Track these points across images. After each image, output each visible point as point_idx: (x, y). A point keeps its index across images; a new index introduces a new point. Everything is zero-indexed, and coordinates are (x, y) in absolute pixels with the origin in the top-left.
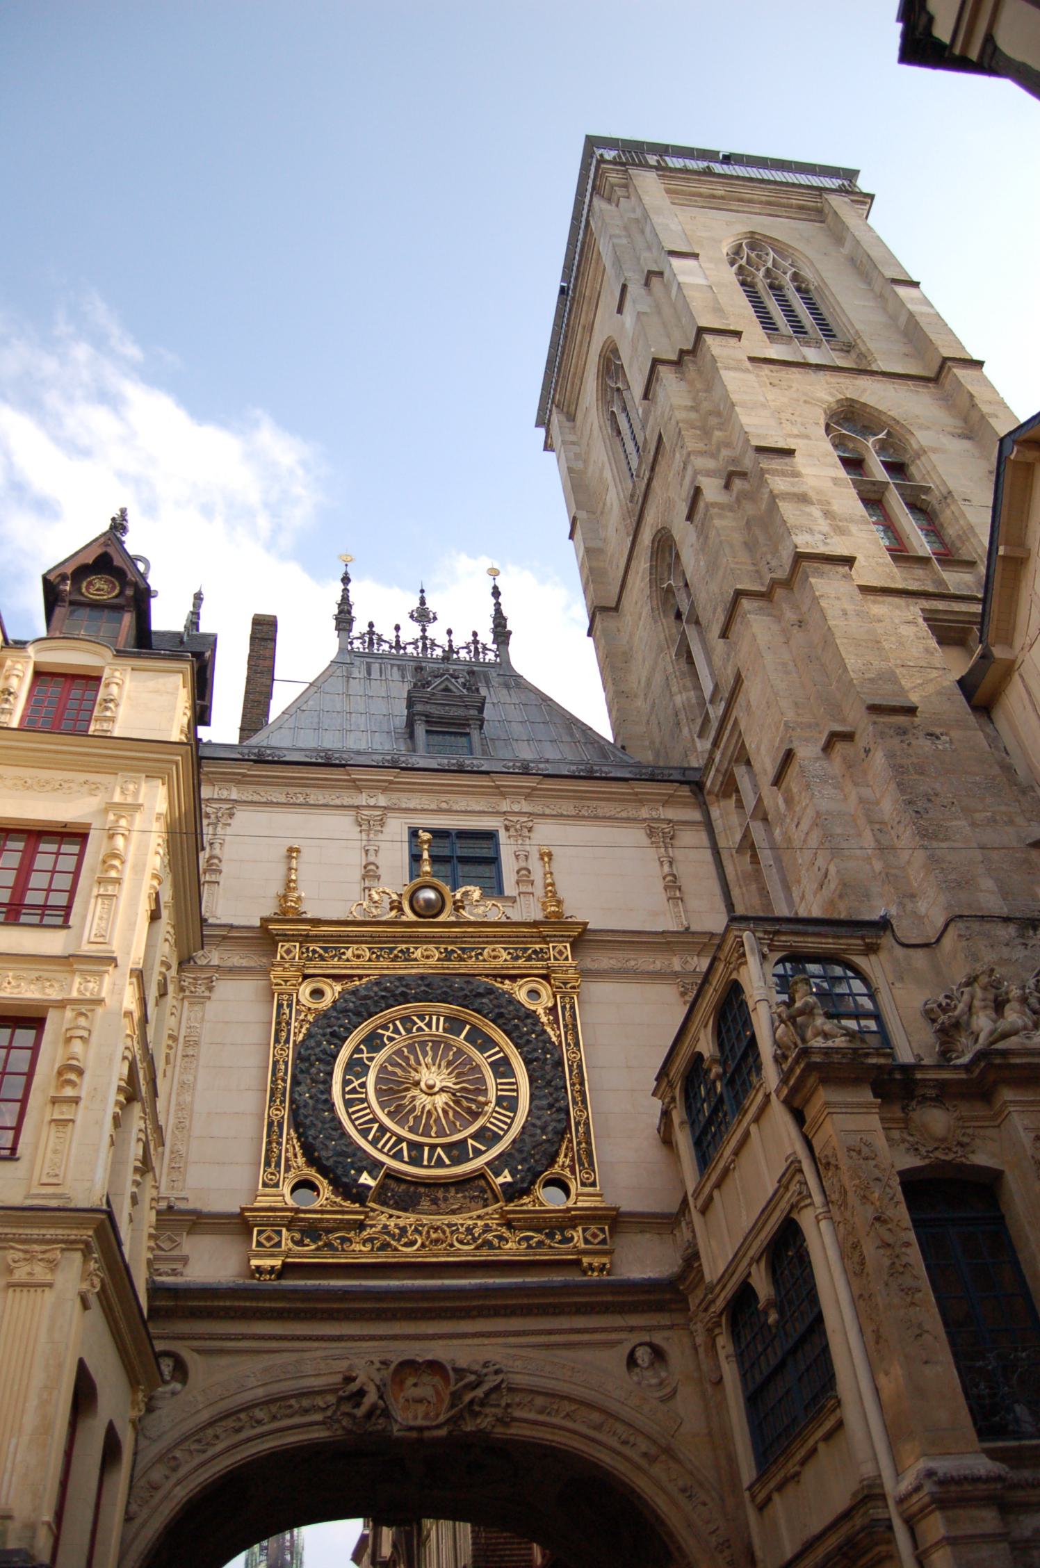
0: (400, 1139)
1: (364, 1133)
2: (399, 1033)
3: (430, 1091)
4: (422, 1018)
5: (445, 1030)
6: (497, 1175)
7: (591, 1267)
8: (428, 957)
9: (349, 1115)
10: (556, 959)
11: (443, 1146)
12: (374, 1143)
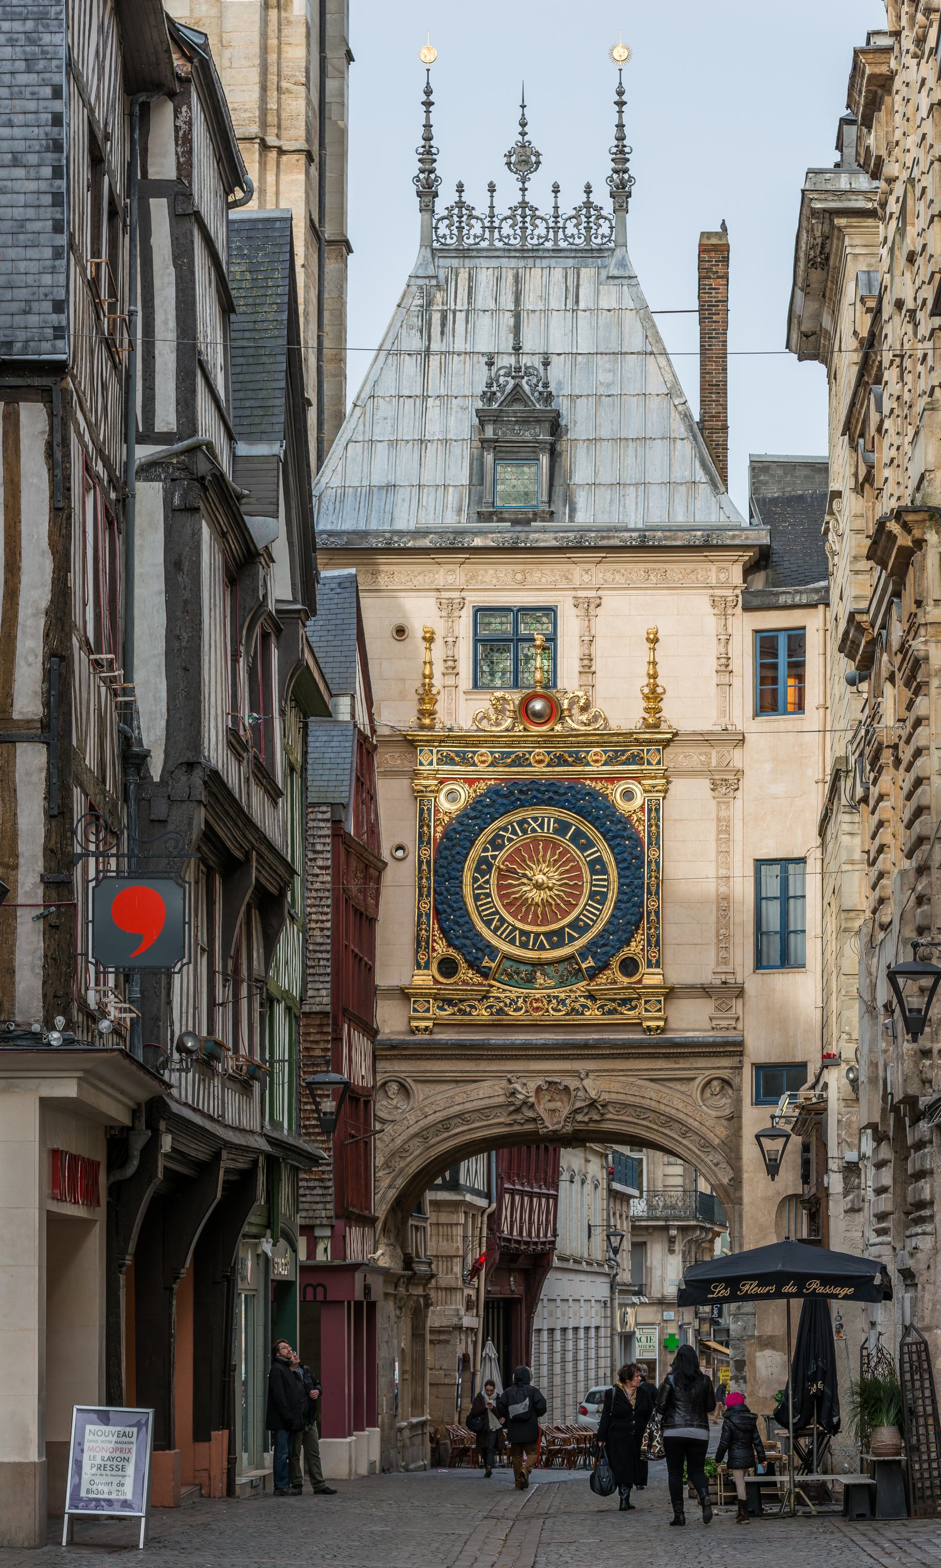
0: (515, 928)
1: (488, 923)
2: (516, 834)
3: (539, 886)
4: (535, 819)
6: (584, 959)
7: (649, 1029)
8: (540, 762)
9: (477, 907)
10: (649, 763)
11: (545, 934)
12: (494, 931)
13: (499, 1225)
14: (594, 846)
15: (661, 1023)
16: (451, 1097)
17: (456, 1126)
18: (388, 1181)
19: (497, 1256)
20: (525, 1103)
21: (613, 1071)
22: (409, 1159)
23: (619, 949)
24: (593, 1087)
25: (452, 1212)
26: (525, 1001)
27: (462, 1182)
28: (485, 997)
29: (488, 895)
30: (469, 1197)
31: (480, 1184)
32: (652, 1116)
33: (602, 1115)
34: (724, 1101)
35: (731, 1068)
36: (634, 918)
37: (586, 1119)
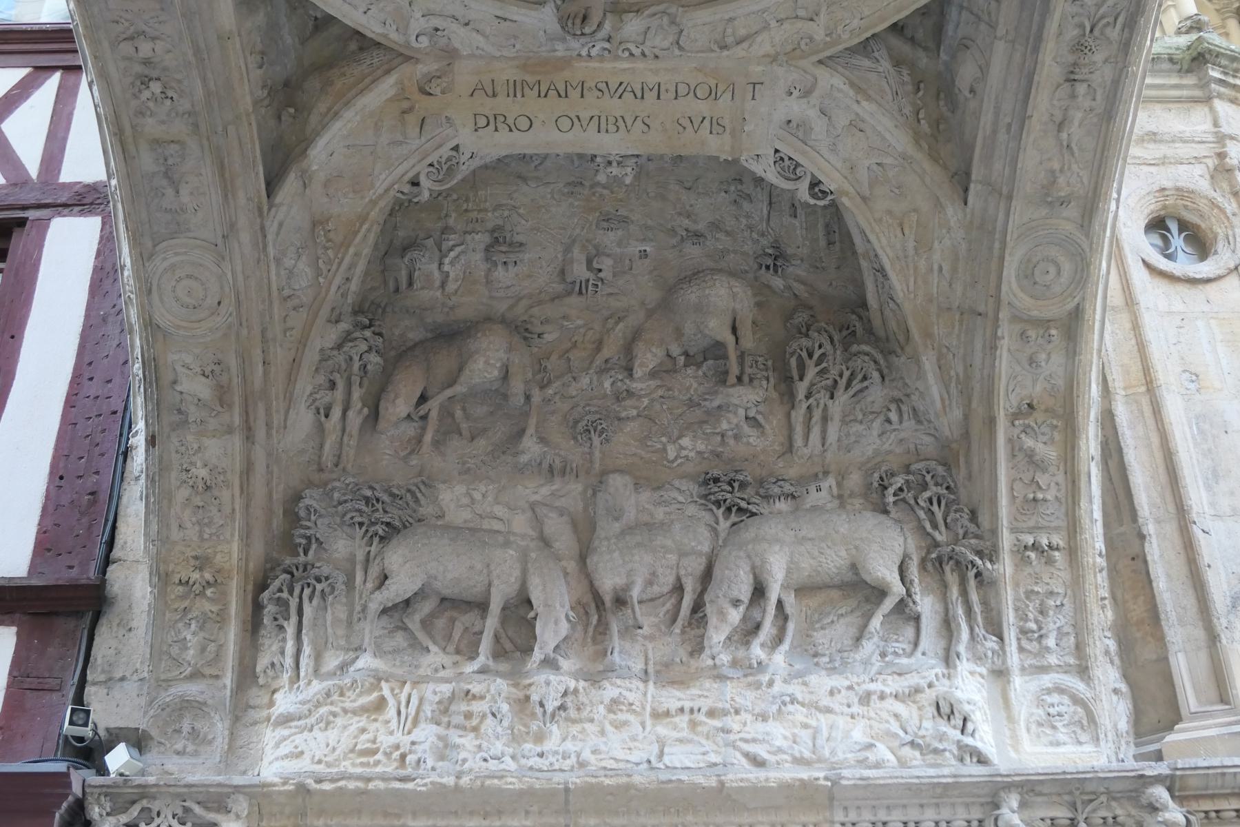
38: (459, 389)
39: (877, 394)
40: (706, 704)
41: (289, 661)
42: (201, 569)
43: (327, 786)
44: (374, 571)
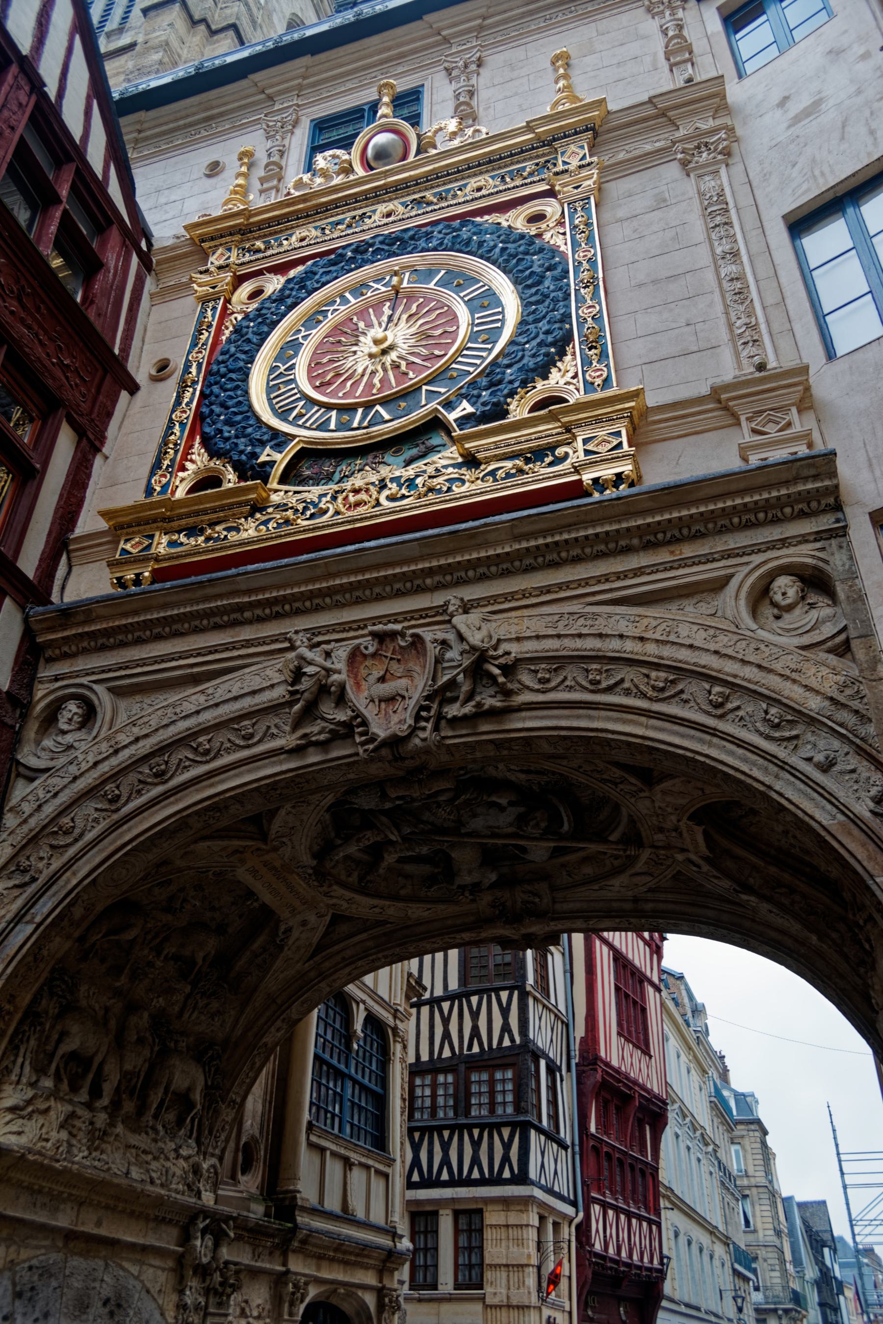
1: (283, 414)
5: (409, 282)
9: (270, 400)
13: (589, 1237)
14: (479, 281)
15: (626, 468)
16: (174, 706)
17: (181, 767)
18: (19, 902)
19: (589, 1273)
20: (323, 690)
21: (525, 594)
22: (71, 851)
23: (524, 383)
24: (475, 628)
25: (521, 1211)
26: (334, 498)
27: (533, 1174)
28: (257, 508)
29: (293, 381)
30: (538, 1193)
31: (563, 1186)
32: (629, 675)
33: (508, 694)
34: (814, 614)
35: (819, 536)
36: (550, 339)
37: (468, 709)
38: (117, 937)
39: (215, 1005)
40: (143, 1146)
41: (17, 1070)
42: (9, 1002)
43: (31, 1157)
44: (59, 1027)
